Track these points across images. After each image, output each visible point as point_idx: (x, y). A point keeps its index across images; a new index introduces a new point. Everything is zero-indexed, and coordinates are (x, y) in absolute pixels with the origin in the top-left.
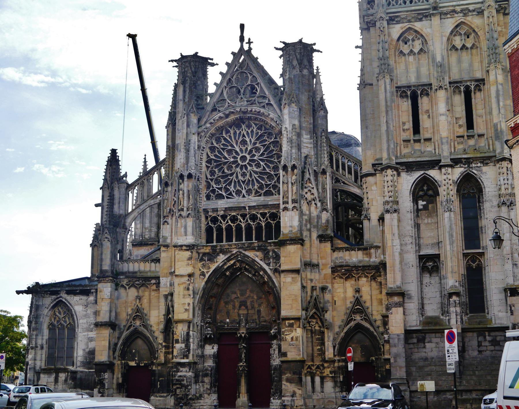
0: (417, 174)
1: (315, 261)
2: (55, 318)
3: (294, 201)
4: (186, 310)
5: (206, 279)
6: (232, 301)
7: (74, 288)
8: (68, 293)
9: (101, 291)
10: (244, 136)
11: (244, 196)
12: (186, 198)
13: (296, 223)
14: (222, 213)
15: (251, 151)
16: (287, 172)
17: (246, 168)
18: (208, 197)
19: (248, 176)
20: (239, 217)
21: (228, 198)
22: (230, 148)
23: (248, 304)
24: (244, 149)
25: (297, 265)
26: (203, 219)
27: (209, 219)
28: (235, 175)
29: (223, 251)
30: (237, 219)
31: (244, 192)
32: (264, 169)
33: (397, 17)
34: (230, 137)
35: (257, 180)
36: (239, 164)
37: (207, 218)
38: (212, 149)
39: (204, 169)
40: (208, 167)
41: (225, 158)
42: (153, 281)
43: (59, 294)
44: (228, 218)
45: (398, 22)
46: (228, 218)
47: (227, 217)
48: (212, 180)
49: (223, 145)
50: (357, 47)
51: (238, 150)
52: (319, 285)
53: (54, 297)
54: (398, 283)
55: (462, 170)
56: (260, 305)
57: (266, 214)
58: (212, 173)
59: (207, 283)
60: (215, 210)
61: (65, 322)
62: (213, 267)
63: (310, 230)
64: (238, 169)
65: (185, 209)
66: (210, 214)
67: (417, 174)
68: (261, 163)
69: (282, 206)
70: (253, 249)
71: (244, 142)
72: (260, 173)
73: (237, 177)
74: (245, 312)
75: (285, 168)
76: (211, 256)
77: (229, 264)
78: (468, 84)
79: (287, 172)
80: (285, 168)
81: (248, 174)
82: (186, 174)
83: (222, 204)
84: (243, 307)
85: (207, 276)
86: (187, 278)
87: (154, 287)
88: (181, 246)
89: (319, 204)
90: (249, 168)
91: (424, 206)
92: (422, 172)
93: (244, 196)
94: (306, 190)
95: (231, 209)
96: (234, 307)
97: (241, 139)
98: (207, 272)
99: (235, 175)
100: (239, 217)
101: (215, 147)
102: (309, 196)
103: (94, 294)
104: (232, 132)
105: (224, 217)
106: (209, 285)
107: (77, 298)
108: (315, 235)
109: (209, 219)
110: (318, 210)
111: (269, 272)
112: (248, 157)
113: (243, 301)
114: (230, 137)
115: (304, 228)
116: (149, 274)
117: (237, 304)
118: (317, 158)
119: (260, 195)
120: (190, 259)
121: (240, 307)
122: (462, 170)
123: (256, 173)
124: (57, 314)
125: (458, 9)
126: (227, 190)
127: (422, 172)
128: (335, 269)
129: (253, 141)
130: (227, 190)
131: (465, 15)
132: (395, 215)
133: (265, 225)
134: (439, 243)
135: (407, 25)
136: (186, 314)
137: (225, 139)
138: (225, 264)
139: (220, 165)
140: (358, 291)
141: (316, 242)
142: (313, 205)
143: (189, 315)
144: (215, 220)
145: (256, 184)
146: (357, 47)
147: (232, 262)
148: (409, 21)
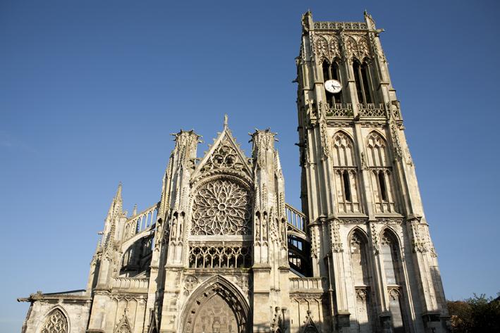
0: (353, 226)
1: (277, 288)
2: (49, 325)
3: (264, 238)
4: (172, 322)
5: (189, 297)
6: (209, 317)
7: (72, 298)
8: (66, 302)
9: (96, 302)
10: (223, 190)
11: (221, 234)
12: (179, 231)
13: (265, 256)
14: (203, 245)
15: (228, 201)
16: (259, 217)
17: (224, 213)
18: (193, 233)
19: (225, 219)
20: (217, 249)
21: (208, 234)
22: (212, 198)
23: (221, 320)
24: (223, 199)
25: (268, 289)
26: (188, 249)
27: (193, 249)
28: (215, 218)
29: (205, 274)
30: (215, 251)
31: (222, 231)
32: (238, 215)
33: (332, 122)
34: (213, 190)
35: (232, 223)
36: (218, 210)
37: (191, 248)
38: (199, 197)
39: (191, 211)
40: (193, 210)
41: (208, 205)
42: (142, 297)
43: (57, 302)
44: (208, 249)
45: (332, 126)
46: (208, 249)
47: (207, 248)
48: (196, 220)
49: (207, 195)
50: (296, 144)
51: (218, 200)
52: (281, 307)
53: (53, 305)
54: (345, 308)
55: (383, 225)
56: (231, 321)
57: (238, 248)
58: (197, 215)
59: (189, 300)
60: (199, 243)
61: (58, 328)
62: (197, 286)
63: (274, 263)
64: (218, 214)
65: (177, 239)
66: (193, 245)
67: (353, 226)
68: (236, 211)
69: (255, 242)
70: (230, 274)
71: (224, 195)
72: (235, 217)
73: (217, 219)
74: (219, 327)
75: (258, 214)
76: (195, 277)
77: (208, 286)
78: (381, 169)
79: (259, 217)
80: (258, 214)
81: (226, 218)
82: (180, 212)
83: (203, 238)
84: (217, 322)
85: (191, 294)
86: (174, 294)
87: (142, 301)
88: (172, 268)
89: (280, 244)
90: (226, 213)
91: (355, 250)
92: (355, 225)
93: (221, 234)
94: (272, 232)
95: (211, 242)
96: (209, 322)
97: (221, 192)
98: (191, 291)
99: (215, 218)
100: (217, 249)
101: (200, 196)
102: (274, 238)
103: (89, 305)
104: (214, 186)
105: (205, 249)
106: (191, 301)
107: (73, 307)
108: (277, 266)
109: (193, 249)
110: (280, 248)
111: (242, 293)
112: (226, 206)
113: (217, 318)
114: (213, 190)
115: (270, 260)
116: (138, 291)
117: (212, 320)
118: (278, 210)
119: (234, 234)
120: (178, 279)
121: (214, 322)
122: (383, 225)
123: (231, 217)
124: (52, 320)
125: (372, 122)
126: (208, 228)
127: (355, 225)
128: (292, 295)
129: (230, 194)
130: (208, 228)
131: (376, 126)
132: (341, 253)
133: (238, 258)
134: (369, 278)
135: (338, 129)
136: (172, 325)
137: (209, 191)
138: (206, 285)
139: (203, 208)
140: (309, 313)
141: (277, 271)
142: (276, 244)
143: (174, 326)
144: (197, 251)
145: (231, 225)
146: (296, 144)
147: (211, 284)
148: (340, 126)
